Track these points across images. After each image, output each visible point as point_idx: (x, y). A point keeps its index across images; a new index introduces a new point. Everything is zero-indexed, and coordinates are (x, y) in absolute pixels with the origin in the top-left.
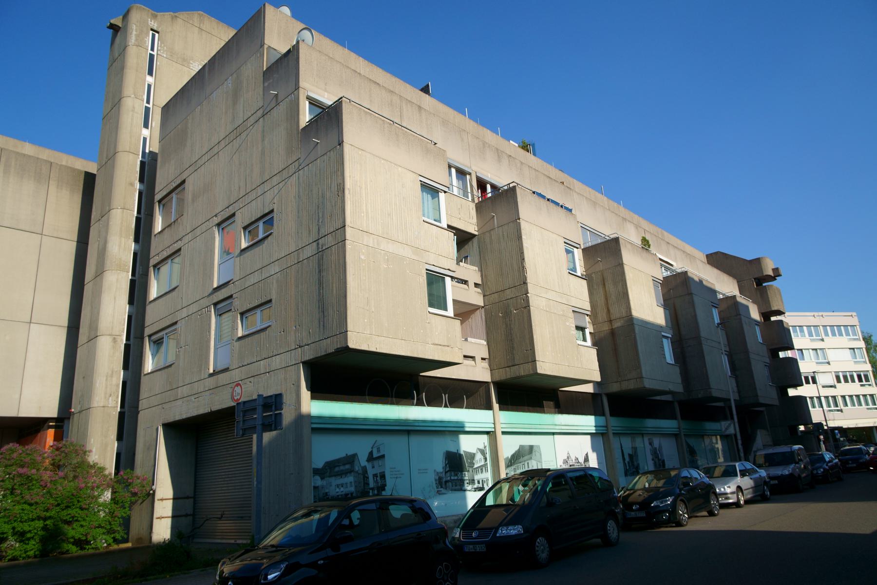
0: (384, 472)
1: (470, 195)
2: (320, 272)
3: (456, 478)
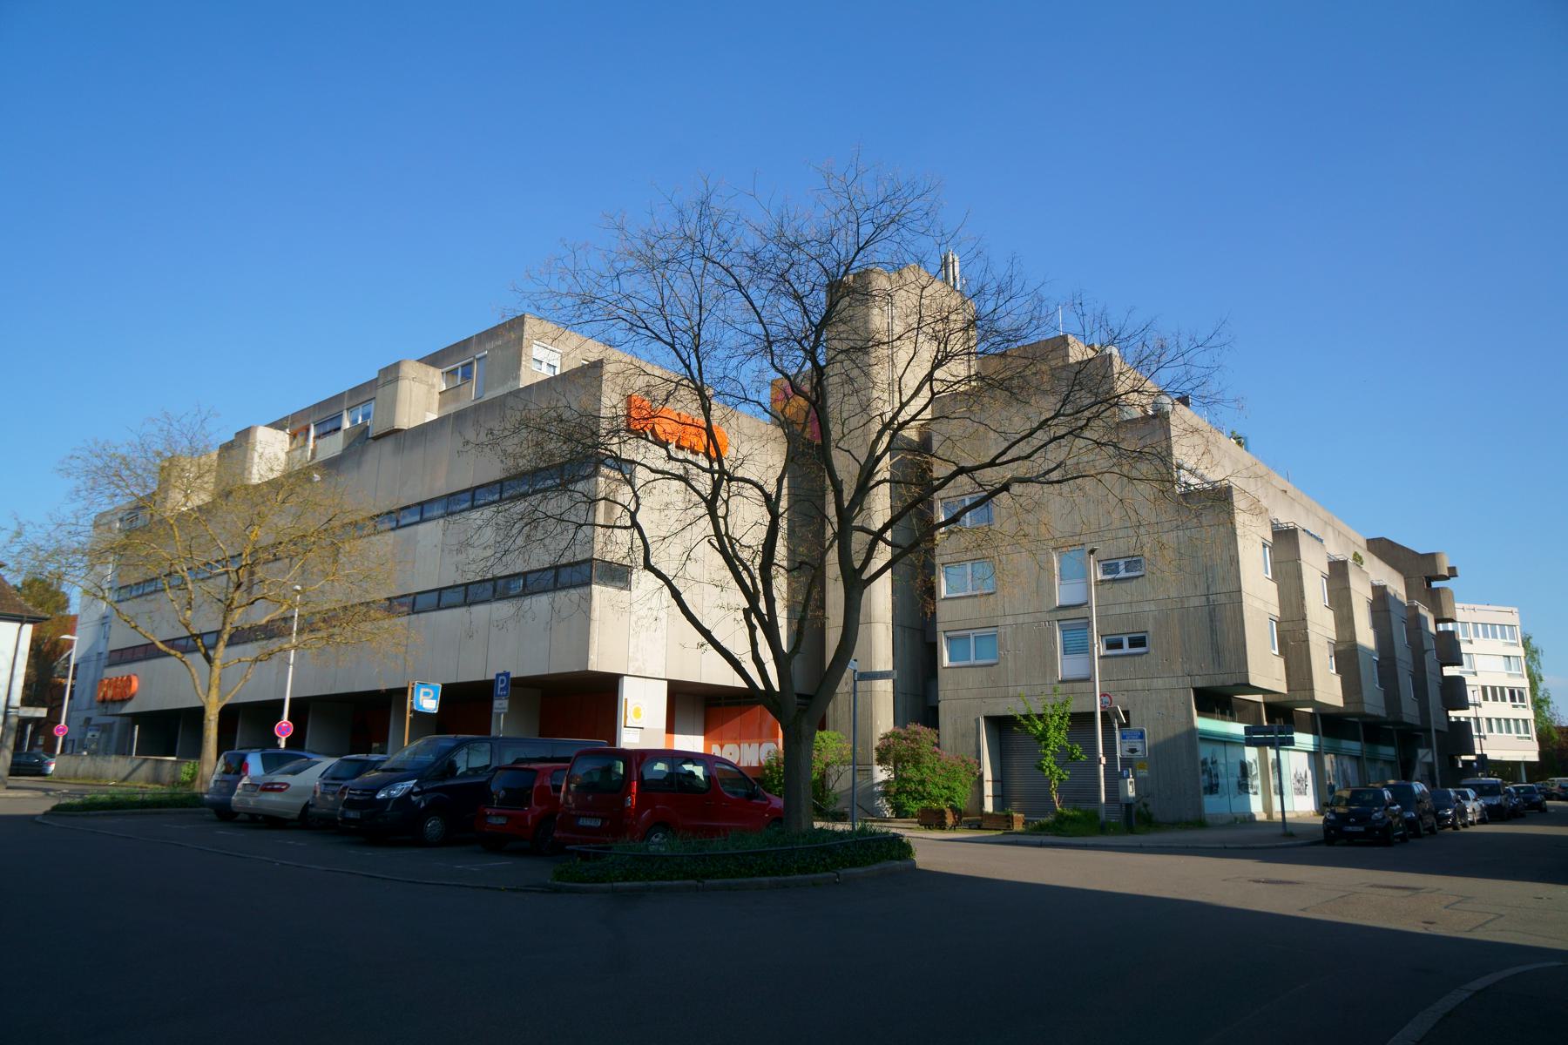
2: (1211, 621)
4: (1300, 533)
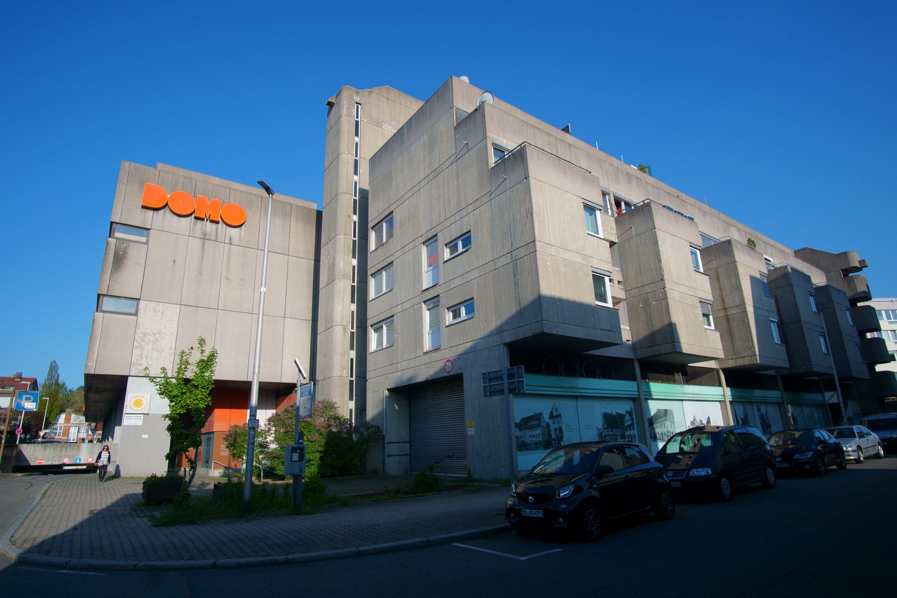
0: (561, 427)
1: (609, 211)
3: (612, 433)
4: (653, 205)
